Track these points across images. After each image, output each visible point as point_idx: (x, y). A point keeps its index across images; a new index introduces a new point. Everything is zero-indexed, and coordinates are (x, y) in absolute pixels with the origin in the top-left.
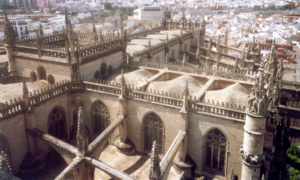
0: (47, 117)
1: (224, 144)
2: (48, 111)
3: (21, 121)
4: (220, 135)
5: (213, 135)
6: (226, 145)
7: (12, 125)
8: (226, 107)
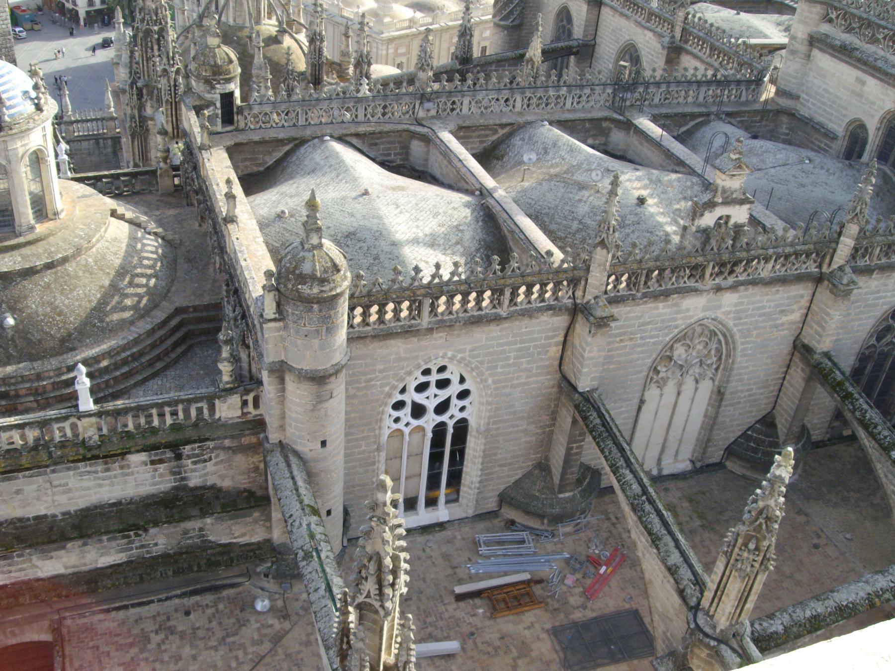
0: (872, 321)
2: (884, 304)
3: (793, 307)
7: (767, 310)
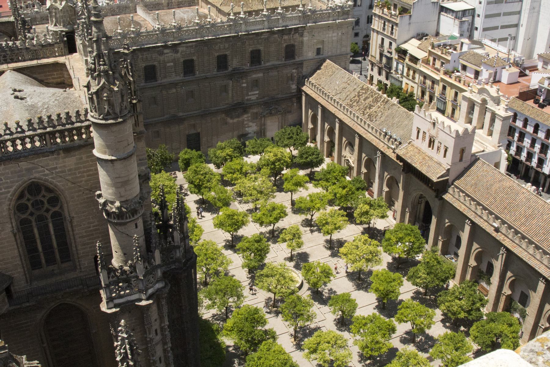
1: (57, 209)
4: (43, 192)
5: (28, 200)
6: (61, 207)
8: (39, 129)
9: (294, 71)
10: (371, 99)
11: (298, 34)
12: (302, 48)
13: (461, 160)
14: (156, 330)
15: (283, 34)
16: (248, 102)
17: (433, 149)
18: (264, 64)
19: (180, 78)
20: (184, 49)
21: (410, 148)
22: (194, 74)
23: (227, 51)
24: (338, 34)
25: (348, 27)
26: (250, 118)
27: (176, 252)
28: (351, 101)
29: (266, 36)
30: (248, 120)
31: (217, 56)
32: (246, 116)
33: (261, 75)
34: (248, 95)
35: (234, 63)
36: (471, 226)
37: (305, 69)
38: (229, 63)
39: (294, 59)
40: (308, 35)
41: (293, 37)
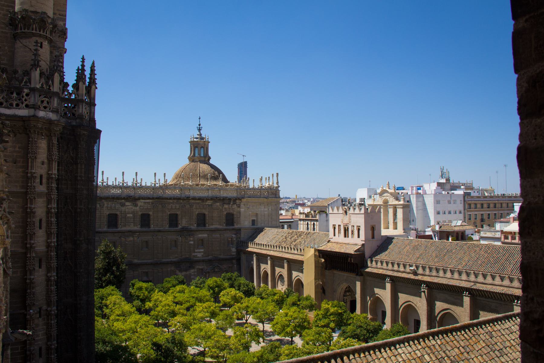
9: (234, 236)
10: (296, 236)
11: (236, 205)
12: (239, 217)
13: (373, 237)
14: (41, 176)
15: (224, 204)
16: (195, 259)
17: (348, 237)
18: (208, 226)
19: (137, 228)
20: (143, 204)
21: (330, 244)
22: (149, 227)
23: (178, 211)
24: (268, 209)
25: (276, 204)
26: (196, 273)
27: (79, 108)
28: (280, 243)
29: (210, 203)
30: (194, 275)
31: (169, 214)
32: (192, 271)
33: (206, 235)
34: (195, 252)
35: (183, 223)
36: (391, 283)
37: (242, 236)
38: (179, 222)
39: (233, 226)
40: (244, 207)
41: (232, 207)
